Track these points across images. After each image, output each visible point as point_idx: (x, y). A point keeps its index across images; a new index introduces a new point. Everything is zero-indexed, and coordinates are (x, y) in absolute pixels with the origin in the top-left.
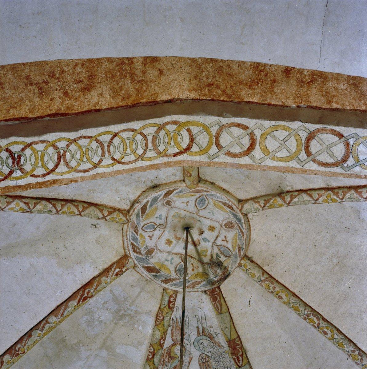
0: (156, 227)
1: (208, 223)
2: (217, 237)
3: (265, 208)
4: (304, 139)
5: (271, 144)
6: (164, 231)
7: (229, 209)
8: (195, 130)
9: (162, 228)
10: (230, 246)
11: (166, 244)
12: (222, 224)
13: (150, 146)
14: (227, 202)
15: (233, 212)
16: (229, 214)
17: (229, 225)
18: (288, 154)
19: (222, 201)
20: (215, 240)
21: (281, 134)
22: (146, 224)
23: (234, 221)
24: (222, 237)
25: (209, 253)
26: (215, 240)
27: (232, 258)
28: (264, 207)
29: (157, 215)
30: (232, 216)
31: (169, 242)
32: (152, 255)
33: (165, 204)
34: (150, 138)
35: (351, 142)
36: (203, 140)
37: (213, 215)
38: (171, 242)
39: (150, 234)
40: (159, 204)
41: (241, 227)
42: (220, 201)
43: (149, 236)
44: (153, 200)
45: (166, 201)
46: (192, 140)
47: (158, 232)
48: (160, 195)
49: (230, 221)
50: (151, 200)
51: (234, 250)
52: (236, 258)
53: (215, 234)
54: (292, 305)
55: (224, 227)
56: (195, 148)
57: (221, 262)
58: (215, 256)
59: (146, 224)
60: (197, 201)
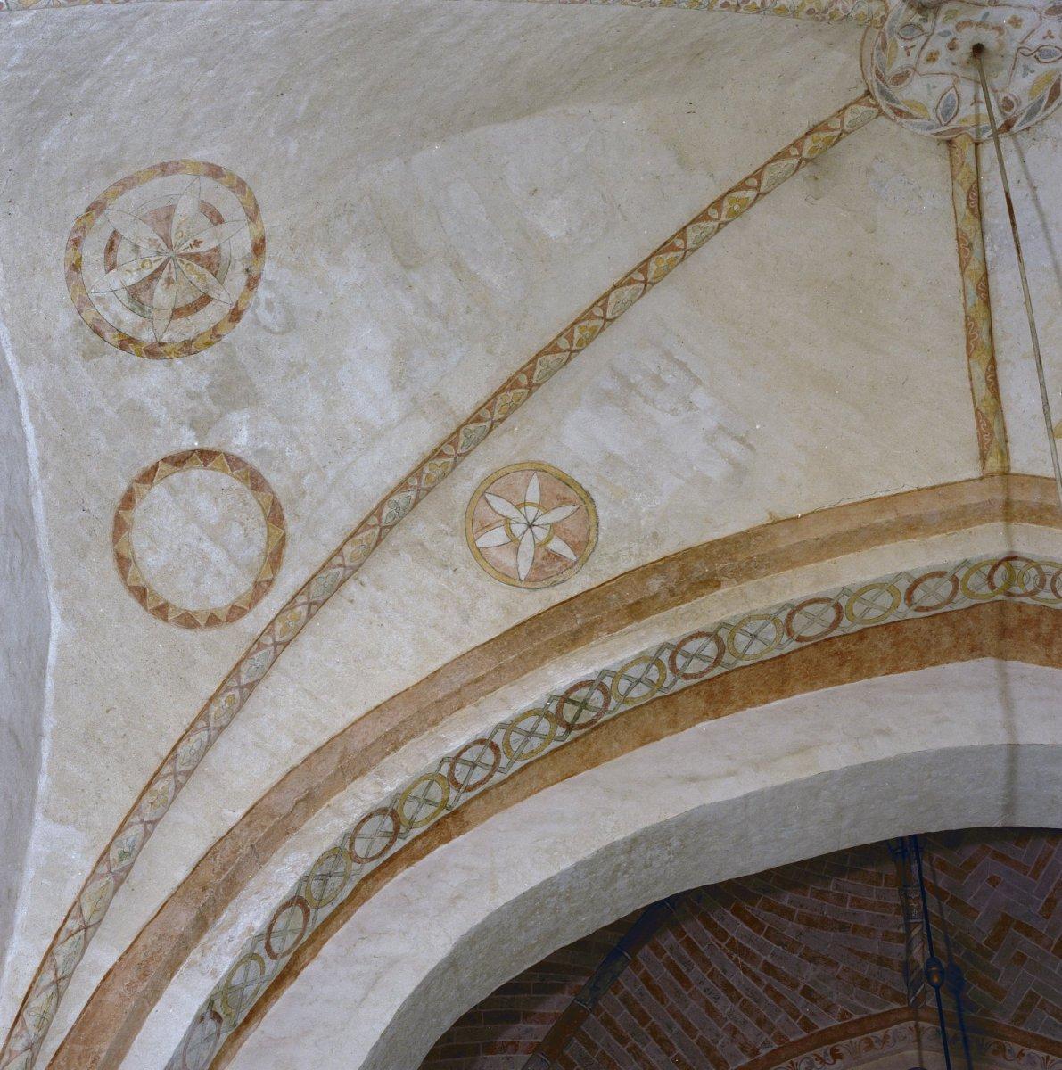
0: (1037, 53)
1: (936, 66)
2: (922, 48)
3: (839, 132)
4: (845, 618)
5: (886, 600)
6: (1022, 42)
7: (901, 107)
8: (986, 590)
9: (1024, 48)
10: (901, 44)
11: (1021, 20)
12: (913, 75)
13: (1049, 579)
14: (904, 121)
15: (893, 105)
16: (900, 99)
17: (900, 78)
18: (863, 596)
19: (914, 121)
20: (927, 41)
21: (874, 613)
22: (1053, 62)
23: (892, 89)
24: (914, 52)
25: (940, 20)
26: (927, 41)
27: (897, 25)
28: (841, 134)
29: (1031, 77)
30: (897, 96)
31: (1016, 22)
32: (1052, 5)
33: (1015, 103)
34: (1048, 586)
35: (785, 638)
36: (976, 581)
37: (929, 85)
38: (1010, 22)
39: (1049, 41)
40: (1026, 103)
41: (881, 83)
42: (916, 118)
43: (1052, 37)
44: (1036, 113)
45: (1013, 110)
46: (990, 578)
47: (1034, 42)
48: (1021, 124)
49: (899, 87)
50: (1040, 112)
51: (895, 41)
52: (891, 29)
53: (928, 49)
54: (790, 13)
55: (910, 70)
56: (987, 570)
57: (920, 13)
58: (931, 16)
59: (1053, 62)
60: (956, 108)
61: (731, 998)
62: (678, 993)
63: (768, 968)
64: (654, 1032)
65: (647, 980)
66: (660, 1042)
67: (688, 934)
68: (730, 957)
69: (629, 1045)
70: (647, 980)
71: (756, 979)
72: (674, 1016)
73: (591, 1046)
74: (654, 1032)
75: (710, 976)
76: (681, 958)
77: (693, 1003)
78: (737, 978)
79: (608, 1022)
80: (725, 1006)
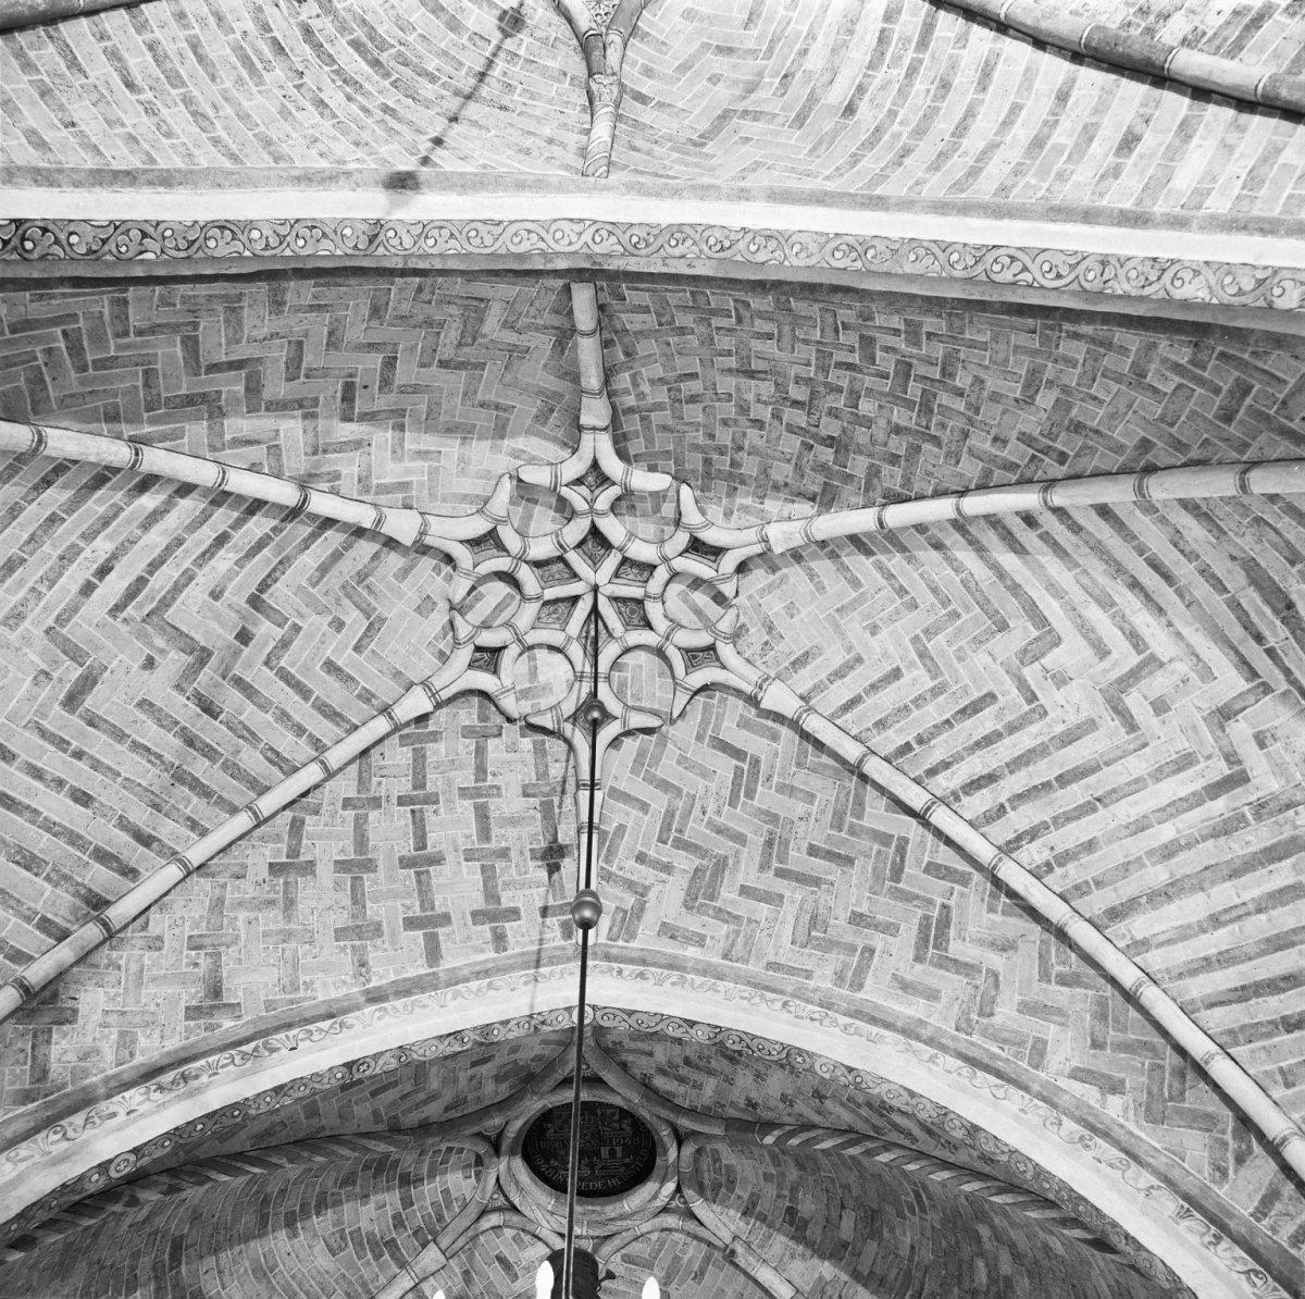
61: (322, 114)
62: (240, 81)
63: (386, 109)
64: (188, 101)
65: (195, 46)
66: (194, 114)
67: (276, 34)
68: (333, 81)
69: (142, 97)
70: (195, 46)
71: (366, 111)
72: (227, 99)
73: (73, 64)
74: (188, 101)
75: (298, 87)
76: (258, 52)
77: (260, 100)
78: (334, 97)
79: (114, 56)
80: (311, 116)
